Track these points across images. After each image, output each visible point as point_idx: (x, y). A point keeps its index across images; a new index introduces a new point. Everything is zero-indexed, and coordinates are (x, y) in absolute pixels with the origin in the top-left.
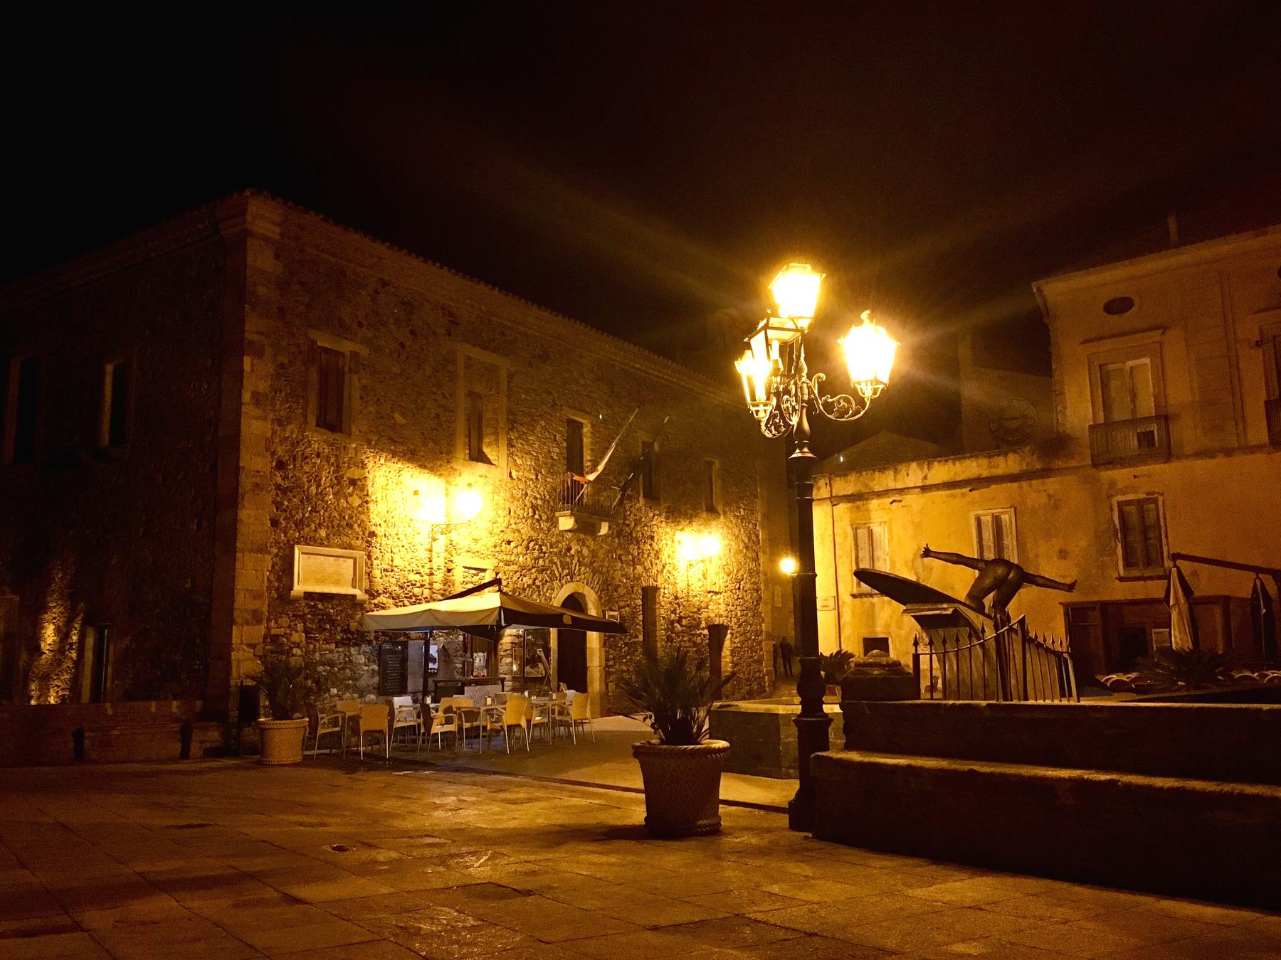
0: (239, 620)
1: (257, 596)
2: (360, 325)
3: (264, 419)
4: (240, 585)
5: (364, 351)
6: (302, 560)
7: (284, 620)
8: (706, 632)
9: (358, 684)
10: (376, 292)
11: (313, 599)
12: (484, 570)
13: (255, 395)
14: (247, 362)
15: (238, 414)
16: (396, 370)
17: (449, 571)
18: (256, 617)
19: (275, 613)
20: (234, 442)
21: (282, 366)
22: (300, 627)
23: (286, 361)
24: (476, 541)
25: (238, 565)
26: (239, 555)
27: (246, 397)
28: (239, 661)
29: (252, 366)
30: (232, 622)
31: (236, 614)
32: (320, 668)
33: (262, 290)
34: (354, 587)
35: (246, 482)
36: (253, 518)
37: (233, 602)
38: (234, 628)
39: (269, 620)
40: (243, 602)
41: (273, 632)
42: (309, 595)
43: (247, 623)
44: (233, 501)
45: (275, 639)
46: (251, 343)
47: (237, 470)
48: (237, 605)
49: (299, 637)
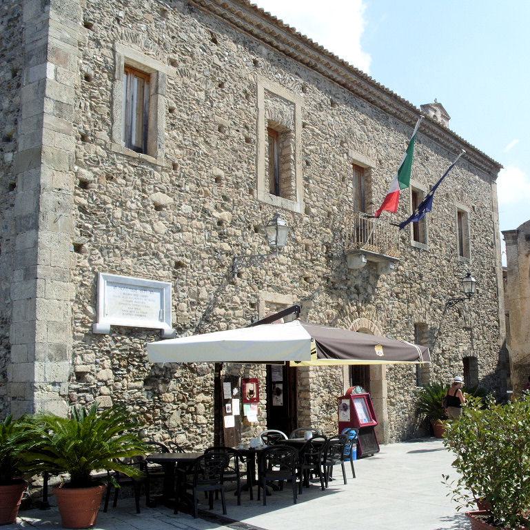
1: (61, 329)
6: (105, 291)
8: (461, 363)
9: (167, 423)
11: (120, 334)
14: (50, 67)
15: (40, 124)
17: (252, 305)
18: (60, 352)
20: (35, 156)
21: (87, 78)
22: (107, 363)
24: (276, 275)
27: (49, 106)
28: (43, 402)
29: (56, 71)
30: (31, 358)
31: (38, 348)
34: (162, 320)
35: (48, 200)
36: (54, 244)
37: (33, 335)
38: (37, 364)
39: (74, 355)
40: (45, 336)
41: (80, 368)
42: (116, 329)
45: (80, 376)
47: (38, 190)
48: (38, 338)
49: (106, 374)
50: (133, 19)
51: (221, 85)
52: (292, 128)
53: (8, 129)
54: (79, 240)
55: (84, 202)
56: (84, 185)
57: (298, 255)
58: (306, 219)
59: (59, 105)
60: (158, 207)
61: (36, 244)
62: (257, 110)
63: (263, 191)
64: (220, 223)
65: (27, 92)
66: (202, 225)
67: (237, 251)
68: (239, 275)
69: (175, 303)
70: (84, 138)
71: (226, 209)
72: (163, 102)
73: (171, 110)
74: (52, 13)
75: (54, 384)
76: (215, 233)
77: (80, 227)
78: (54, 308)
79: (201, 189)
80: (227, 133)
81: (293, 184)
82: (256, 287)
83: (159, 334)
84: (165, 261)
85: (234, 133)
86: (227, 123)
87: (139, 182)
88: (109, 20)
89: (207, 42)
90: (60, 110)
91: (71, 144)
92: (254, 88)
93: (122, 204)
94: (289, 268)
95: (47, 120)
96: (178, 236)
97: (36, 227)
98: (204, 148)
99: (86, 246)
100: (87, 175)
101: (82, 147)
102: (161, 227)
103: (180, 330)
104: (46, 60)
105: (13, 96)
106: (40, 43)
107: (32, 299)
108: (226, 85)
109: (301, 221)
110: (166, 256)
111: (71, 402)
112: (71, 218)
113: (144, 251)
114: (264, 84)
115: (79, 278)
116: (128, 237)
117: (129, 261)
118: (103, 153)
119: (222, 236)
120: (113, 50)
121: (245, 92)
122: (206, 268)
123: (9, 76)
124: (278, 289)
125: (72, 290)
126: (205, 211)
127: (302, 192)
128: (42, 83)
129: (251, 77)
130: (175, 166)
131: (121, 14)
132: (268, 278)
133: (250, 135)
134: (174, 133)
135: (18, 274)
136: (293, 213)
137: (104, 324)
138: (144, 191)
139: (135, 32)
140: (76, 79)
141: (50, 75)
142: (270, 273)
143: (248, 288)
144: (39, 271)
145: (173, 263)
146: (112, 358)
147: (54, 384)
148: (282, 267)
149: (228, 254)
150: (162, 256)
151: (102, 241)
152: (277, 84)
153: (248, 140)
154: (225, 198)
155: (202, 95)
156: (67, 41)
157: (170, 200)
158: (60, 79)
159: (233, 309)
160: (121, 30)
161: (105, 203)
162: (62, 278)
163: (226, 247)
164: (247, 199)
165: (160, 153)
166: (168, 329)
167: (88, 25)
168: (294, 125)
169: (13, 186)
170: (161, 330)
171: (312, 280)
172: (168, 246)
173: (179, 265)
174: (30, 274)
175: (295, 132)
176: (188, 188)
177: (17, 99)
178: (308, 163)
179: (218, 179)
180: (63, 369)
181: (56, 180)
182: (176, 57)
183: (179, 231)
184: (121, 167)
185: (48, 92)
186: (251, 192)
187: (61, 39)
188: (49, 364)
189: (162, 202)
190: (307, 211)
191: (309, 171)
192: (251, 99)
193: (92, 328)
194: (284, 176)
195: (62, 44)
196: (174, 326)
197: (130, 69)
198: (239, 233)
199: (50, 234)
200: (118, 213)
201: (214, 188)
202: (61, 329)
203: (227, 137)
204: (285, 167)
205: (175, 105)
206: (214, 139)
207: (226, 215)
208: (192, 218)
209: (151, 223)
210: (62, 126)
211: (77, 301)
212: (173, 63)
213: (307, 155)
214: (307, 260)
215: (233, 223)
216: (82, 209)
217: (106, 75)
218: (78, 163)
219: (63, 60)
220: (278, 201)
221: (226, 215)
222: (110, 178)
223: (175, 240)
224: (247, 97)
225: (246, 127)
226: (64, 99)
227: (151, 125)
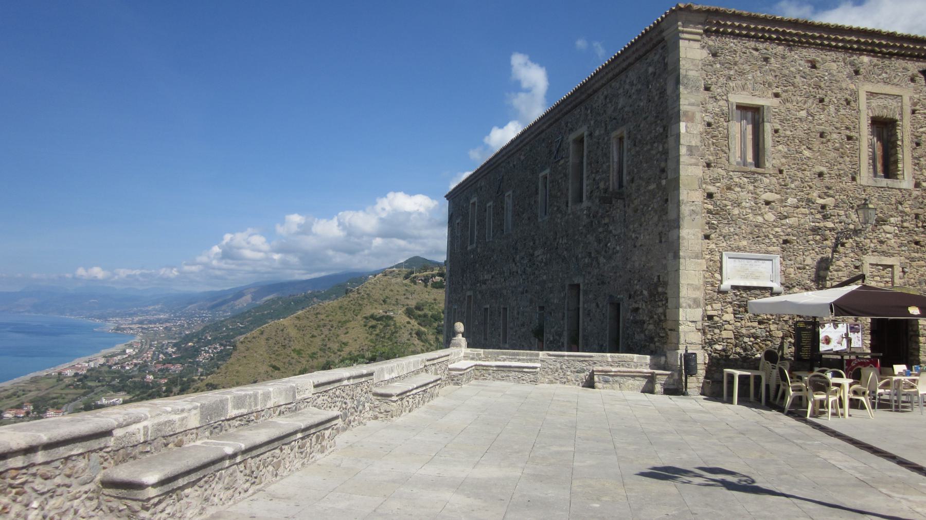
0: (684, 305)
1: (696, 288)
2: (770, 85)
3: (696, 165)
4: (683, 281)
5: (776, 101)
7: (718, 306)
10: (784, 57)
12: (891, 266)
13: (690, 149)
14: (683, 125)
16: (803, 114)
17: (856, 267)
18: (696, 303)
19: (710, 301)
20: (675, 183)
21: (709, 125)
22: (730, 310)
23: (712, 121)
24: (882, 242)
25: (681, 267)
26: (682, 260)
27: (683, 150)
28: (685, 333)
29: (686, 127)
30: (678, 307)
31: (682, 300)
32: (746, 340)
33: (692, 73)
35: (685, 210)
36: (690, 235)
38: (681, 310)
41: (709, 313)
42: (734, 287)
43: (690, 307)
44: (676, 224)
45: (710, 318)
46: (686, 113)
48: (682, 294)
49: (729, 317)
50: (742, 73)
51: (822, 100)
52: (898, 117)
53: (663, 165)
54: (708, 232)
55: (711, 207)
56: (710, 196)
57: (905, 224)
58: (916, 193)
59: (690, 149)
60: (767, 203)
61: (679, 237)
62: (859, 111)
63: (865, 177)
64: (823, 207)
65: (671, 140)
66: (807, 211)
67: (840, 227)
68: (843, 245)
69: (783, 269)
70: (708, 165)
71: (829, 196)
72: (768, 128)
73: (776, 131)
74: (682, 88)
75: (692, 322)
76: (819, 216)
77: (708, 223)
78: (691, 277)
79: (806, 184)
80: (828, 137)
81: (900, 165)
82: (860, 253)
83: (771, 291)
84: (774, 240)
85: (835, 136)
86: (828, 129)
87: (751, 188)
88: (722, 80)
89: (807, 70)
90: (691, 151)
91: (699, 171)
92: (855, 94)
93: (739, 205)
94: (896, 235)
95: (682, 159)
96: (784, 222)
97: (678, 227)
98: (807, 153)
99: (713, 236)
100: (712, 189)
101: (707, 172)
102: (770, 217)
103: (789, 287)
104: (679, 122)
105: (665, 143)
106: (676, 110)
107: (678, 270)
108: (827, 100)
109: (910, 195)
110: (775, 236)
111: (704, 333)
112: (701, 220)
113: (758, 236)
114: (864, 88)
115: (708, 257)
116: (743, 227)
117: (744, 243)
118: (723, 173)
119: (825, 217)
120: (727, 101)
121: (846, 100)
122: (811, 242)
123: (661, 130)
124: (884, 253)
125: (703, 264)
126: (809, 201)
127: (911, 170)
128: (678, 135)
129: (852, 86)
130: (781, 172)
131: (732, 72)
132: (872, 245)
133: (852, 134)
134: (780, 147)
135: (671, 255)
136: (900, 189)
137: (726, 285)
138: (756, 193)
139: (743, 82)
140: (701, 127)
141: (683, 129)
142: (875, 241)
143: (852, 255)
144: (681, 254)
145: (781, 241)
146: (733, 306)
147: (692, 322)
148: (888, 236)
149: (831, 230)
150: (771, 236)
151: (725, 230)
152: (881, 84)
153: (849, 138)
154: (829, 188)
155: (803, 114)
156: (693, 105)
157: (778, 196)
158: (689, 132)
159: (836, 271)
160: (732, 84)
161: (726, 206)
162: (697, 257)
163: (830, 225)
164: (850, 185)
165: (767, 164)
166: (776, 286)
167: (707, 89)
168: (901, 115)
169: (667, 200)
170: (771, 289)
171: (922, 243)
172: (777, 229)
173: (785, 242)
174: (677, 256)
175: (902, 120)
176: (793, 186)
177: (666, 146)
178: (918, 144)
179: (821, 175)
180: (698, 314)
181: (690, 197)
182: (779, 90)
183: (786, 217)
184: (737, 180)
185: (682, 141)
186: (854, 179)
187: (689, 105)
188: (689, 310)
189: (770, 200)
190: (917, 185)
191: (920, 151)
192: (853, 104)
193: (719, 287)
194: (892, 159)
195: (690, 107)
196: (782, 284)
197: (740, 107)
198: (842, 213)
199: (687, 231)
200: (736, 211)
201: (817, 181)
202: (696, 288)
203: (829, 141)
204: (893, 151)
205: (779, 127)
206: (816, 144)
207: (829, 201)
208: (798, 207)
209: (762, 215)
210: (693, 161)
211: (708, 270)
212: (777, 95)
213: (917, 137)
214: (918, 227)
215: (836, 206)
216: (709, 212)
217: (722, 120)
218: (705, 183)
219: (691, 119)
220: (884, 182)
221: (829, 201)
222: (729, 188)
223: (783, 225)
224: (848, 103)
225: (847, 128)
226: (693, 144)
227: (761, 146)
